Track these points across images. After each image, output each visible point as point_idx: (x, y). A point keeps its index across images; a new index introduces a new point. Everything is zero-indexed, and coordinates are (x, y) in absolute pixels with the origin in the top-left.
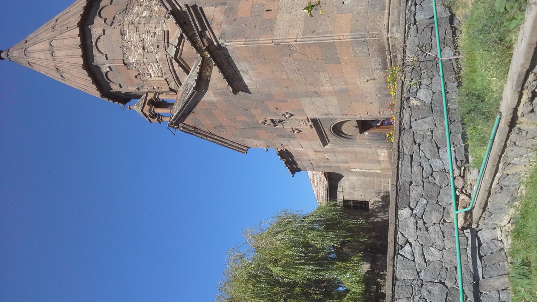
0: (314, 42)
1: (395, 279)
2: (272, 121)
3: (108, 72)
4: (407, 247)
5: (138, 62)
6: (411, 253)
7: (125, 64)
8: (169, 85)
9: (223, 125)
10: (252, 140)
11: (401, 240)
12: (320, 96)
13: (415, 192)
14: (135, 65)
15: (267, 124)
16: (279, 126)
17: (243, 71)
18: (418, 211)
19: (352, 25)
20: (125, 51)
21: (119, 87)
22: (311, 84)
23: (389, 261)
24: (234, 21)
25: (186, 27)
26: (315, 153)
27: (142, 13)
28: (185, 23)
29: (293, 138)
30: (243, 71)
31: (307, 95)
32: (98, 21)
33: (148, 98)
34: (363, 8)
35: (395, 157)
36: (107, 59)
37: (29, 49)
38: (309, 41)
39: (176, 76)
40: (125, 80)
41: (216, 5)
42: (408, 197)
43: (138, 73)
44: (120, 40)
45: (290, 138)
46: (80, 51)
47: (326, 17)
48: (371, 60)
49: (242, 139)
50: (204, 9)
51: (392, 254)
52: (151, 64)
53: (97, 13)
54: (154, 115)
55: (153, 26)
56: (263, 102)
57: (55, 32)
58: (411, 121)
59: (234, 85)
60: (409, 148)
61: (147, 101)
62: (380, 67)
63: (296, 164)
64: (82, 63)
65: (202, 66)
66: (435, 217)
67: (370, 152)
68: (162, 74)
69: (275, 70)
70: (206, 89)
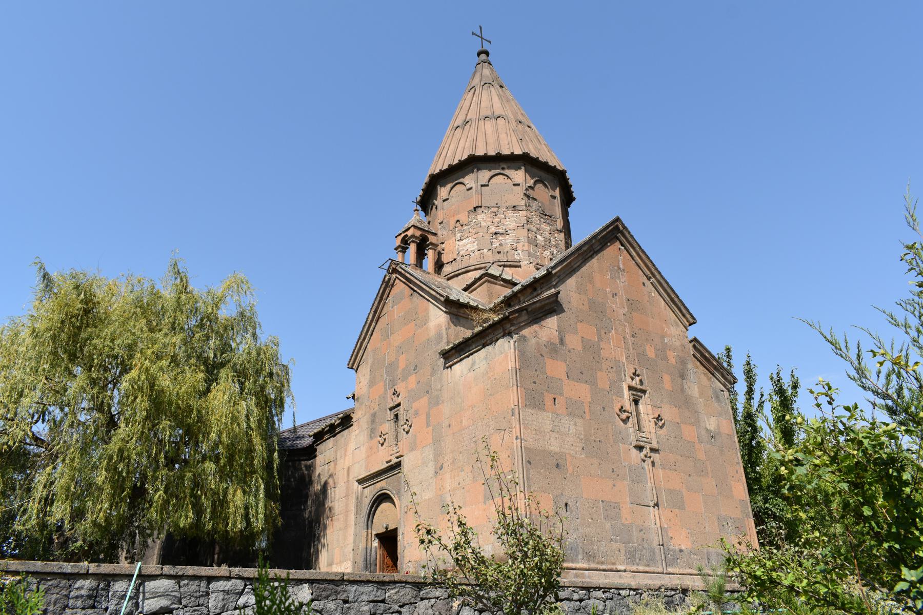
0: (516, 464)
1: (210, 579)
2: (399, 405)
5: (479, 225)
6: (247, 604)
7: (475, 209)
8: (447, 263)
10: (368, 377)
14: (474, 221)
15: (394, 398)
16: (390, 415)
20: (492, 209)
21: (444, 199)
22: (454, 459)
23: (236, 570)
24: (541, 355)
25: (529, 291)
26: (346, 467)
27: (541, 235)
28: (535, 289)
29: (371, 435)
30: (473, 364)
31: (438, 455)
35: (382, 577)
36: (482, 186)
37: (492, 89)
38: (518, 456)
39: (460, 274)
40: (454, 207)
41: (560, 331)
42: (327, 597)
44: (507, 204)
45: (371, 431)
46: (492, 153)
47: (548, 480)
48: (490, 545)
49: (370, 361)
51: (246, 575)
52: (476, 242)
54: (405, 242)
55: (526, 248)
56: (427, 392)
57: (515, 124)
58: (431, 598)
59: (453, 351)
60: (395, 597)
64: (477, 154)
67: (346, 550)
68: (463, 256)
69: (474, 409)
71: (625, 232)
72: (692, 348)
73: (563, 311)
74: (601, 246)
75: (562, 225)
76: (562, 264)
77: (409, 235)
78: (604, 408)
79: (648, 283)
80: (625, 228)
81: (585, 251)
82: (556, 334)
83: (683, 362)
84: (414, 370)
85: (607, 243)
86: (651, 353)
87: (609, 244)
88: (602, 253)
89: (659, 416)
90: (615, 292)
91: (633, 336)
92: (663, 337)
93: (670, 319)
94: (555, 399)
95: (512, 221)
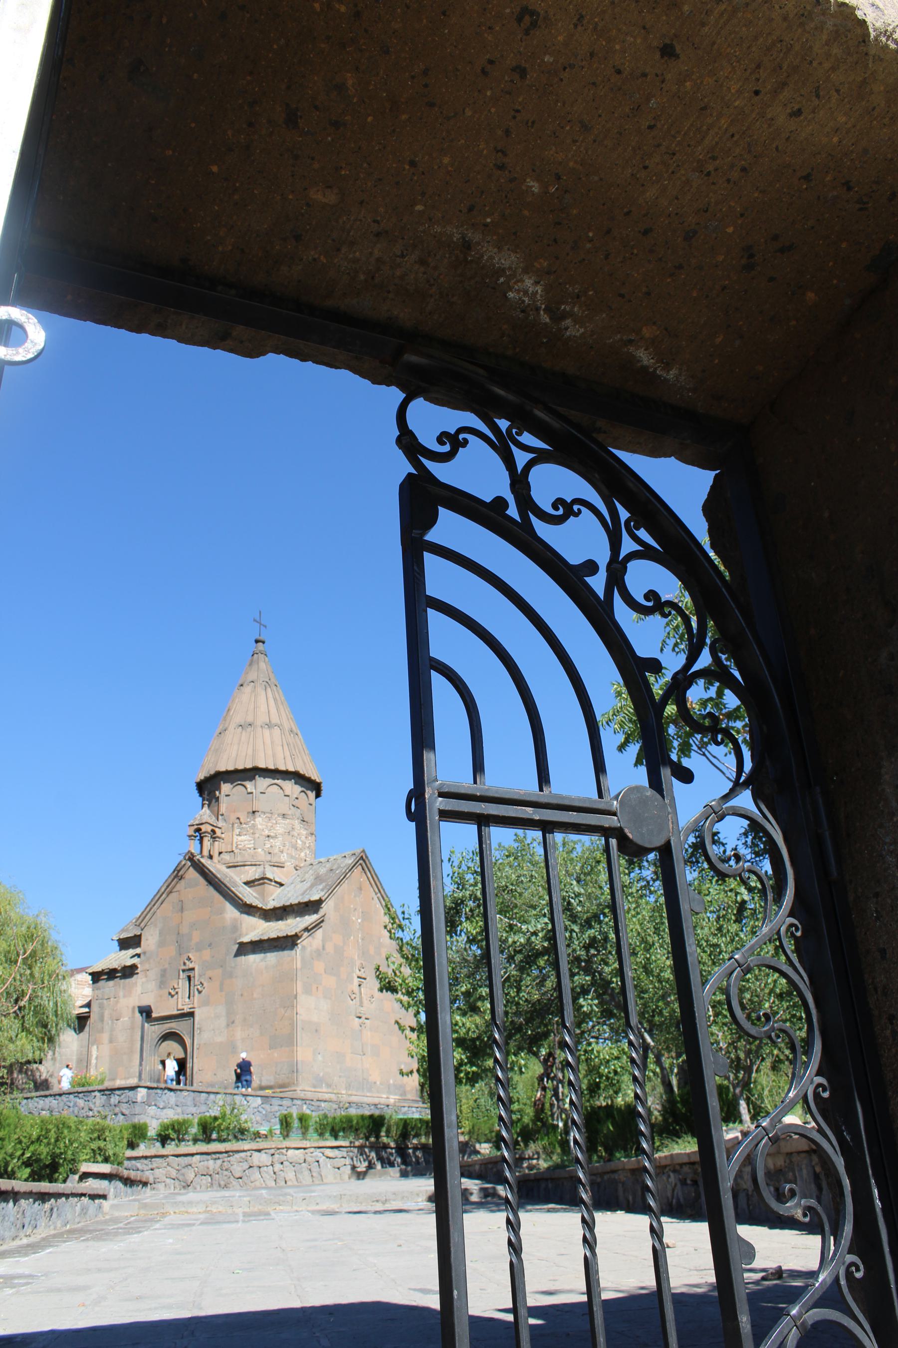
1: (235, 1094)
3: (246, 789)
4: (245, 1102)
7: (254, 812)
9: (185, 913)
11: (249, 1098)
12: (228, 1025)
13: (267, 1107)
17: (265, 958)
18: (260, 1109)
21: (227, 794)
24: (313, 959)
32: (298, 788)
33: (217, 830)
37: (269, 690)
41: (324, 941)
43: (243, 822)
46: (272, 767)
50: (321, 930)
52: (252, 842)
53: (303, 789)
55: (289, 852)
56: (222, 966)
61: (214, 828)
62: (264, 1084)
63: (108, 979)
65: (261, 909)
66: (258, 1118)
70: (242, 912)
77: (203, 830)
79: (375, 898)
80: (367, 857)
82: (321, 943)
84: (209, 946)
86: (372, 952)
91: (363, 939)
95: (281, 827)
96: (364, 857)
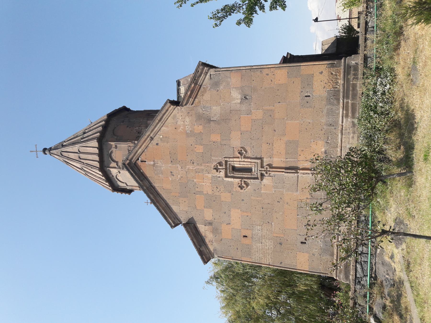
19: (309, 263)
24: (221, 240)
34: (317, 250)
36: (127, 185)
71: (129, 159)
72: (188, 106)
73: (192, 218)
74: (145, 180)
75: (130, 143)
76: (167, 217)
78: (243, 200)
81: (152, 194)
82: (207, 227)
83: (200, 117)
85: (141, 172)
86: (200, 149)
87: (142, 171)
88: (150, 179)
89: (239, 153)
90: (170, 174)
91: (193, 163)
92: (188, 135)
93: (173, 123)
94: (244, 236)
96: (128, 162)
